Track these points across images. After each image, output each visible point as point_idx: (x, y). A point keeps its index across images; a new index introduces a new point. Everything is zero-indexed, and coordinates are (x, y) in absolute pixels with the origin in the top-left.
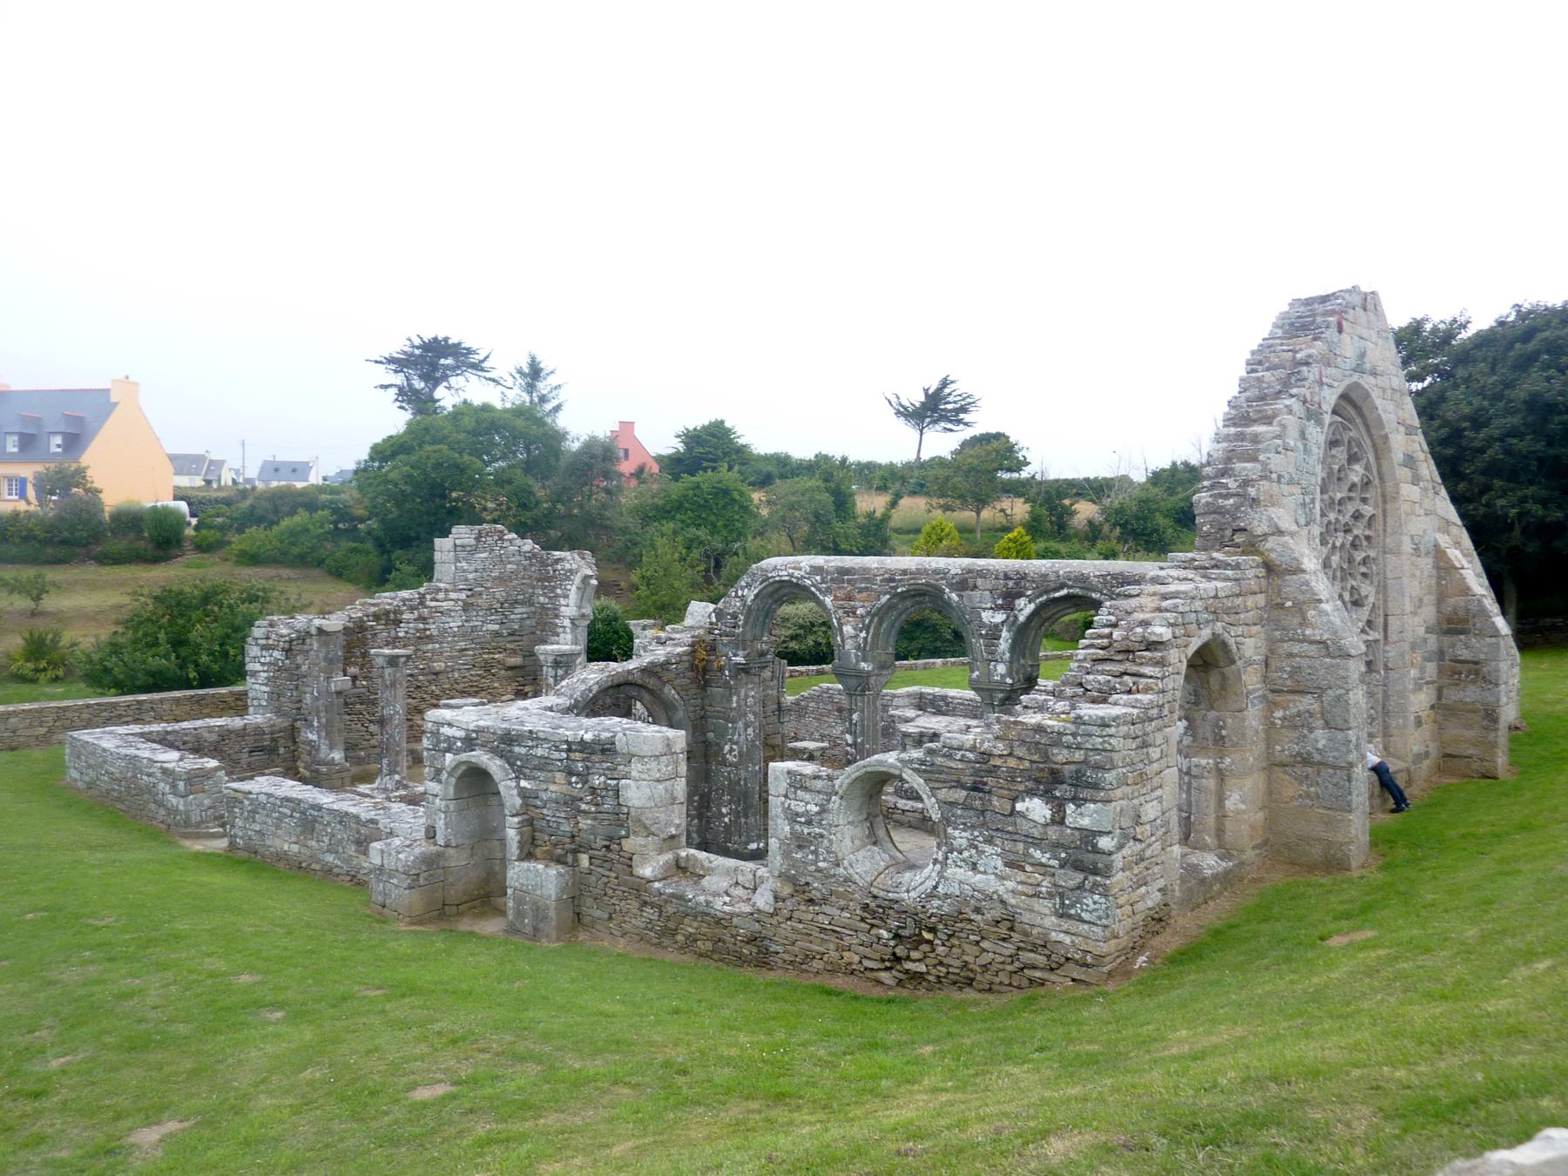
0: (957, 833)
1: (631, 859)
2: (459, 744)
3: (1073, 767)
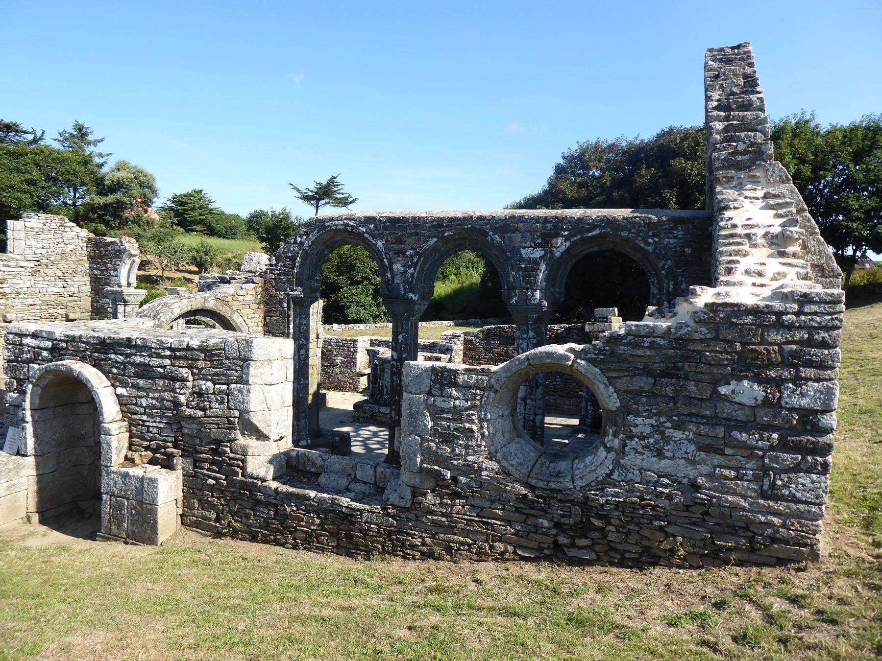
2: (45, 354)
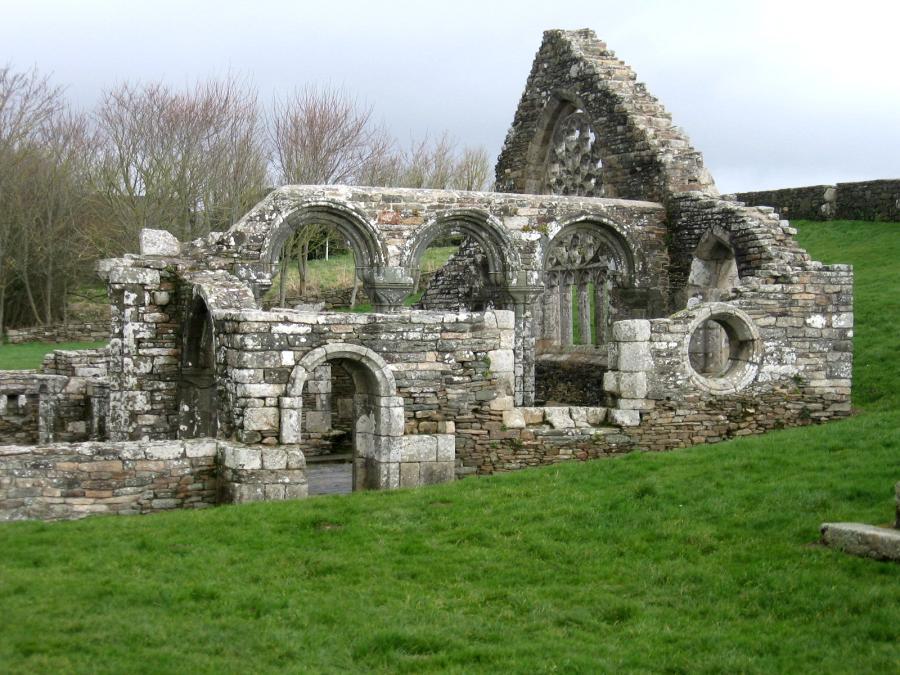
1: (501, 416)
2: (303, 340)
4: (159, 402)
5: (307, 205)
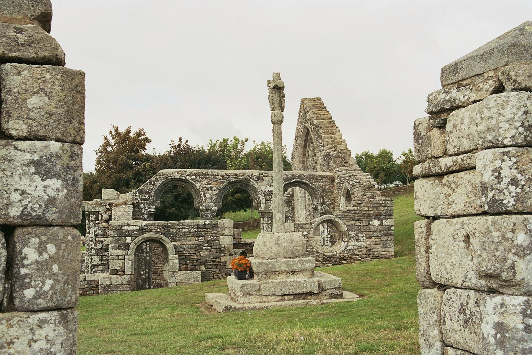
0: (351, 233)
1: (226, 263)
3: (385, 211)
4: (105, 261)
5: (170, 178)
